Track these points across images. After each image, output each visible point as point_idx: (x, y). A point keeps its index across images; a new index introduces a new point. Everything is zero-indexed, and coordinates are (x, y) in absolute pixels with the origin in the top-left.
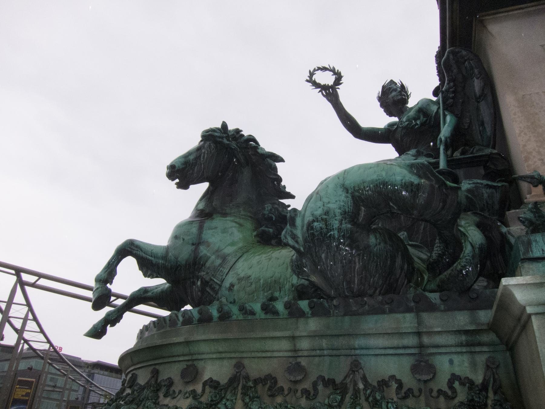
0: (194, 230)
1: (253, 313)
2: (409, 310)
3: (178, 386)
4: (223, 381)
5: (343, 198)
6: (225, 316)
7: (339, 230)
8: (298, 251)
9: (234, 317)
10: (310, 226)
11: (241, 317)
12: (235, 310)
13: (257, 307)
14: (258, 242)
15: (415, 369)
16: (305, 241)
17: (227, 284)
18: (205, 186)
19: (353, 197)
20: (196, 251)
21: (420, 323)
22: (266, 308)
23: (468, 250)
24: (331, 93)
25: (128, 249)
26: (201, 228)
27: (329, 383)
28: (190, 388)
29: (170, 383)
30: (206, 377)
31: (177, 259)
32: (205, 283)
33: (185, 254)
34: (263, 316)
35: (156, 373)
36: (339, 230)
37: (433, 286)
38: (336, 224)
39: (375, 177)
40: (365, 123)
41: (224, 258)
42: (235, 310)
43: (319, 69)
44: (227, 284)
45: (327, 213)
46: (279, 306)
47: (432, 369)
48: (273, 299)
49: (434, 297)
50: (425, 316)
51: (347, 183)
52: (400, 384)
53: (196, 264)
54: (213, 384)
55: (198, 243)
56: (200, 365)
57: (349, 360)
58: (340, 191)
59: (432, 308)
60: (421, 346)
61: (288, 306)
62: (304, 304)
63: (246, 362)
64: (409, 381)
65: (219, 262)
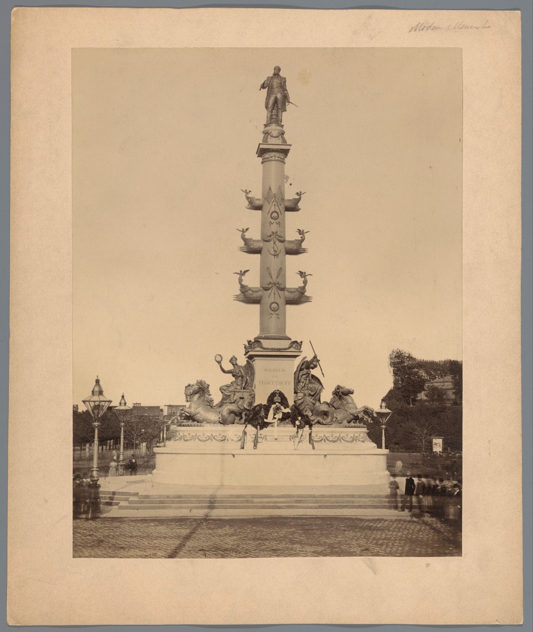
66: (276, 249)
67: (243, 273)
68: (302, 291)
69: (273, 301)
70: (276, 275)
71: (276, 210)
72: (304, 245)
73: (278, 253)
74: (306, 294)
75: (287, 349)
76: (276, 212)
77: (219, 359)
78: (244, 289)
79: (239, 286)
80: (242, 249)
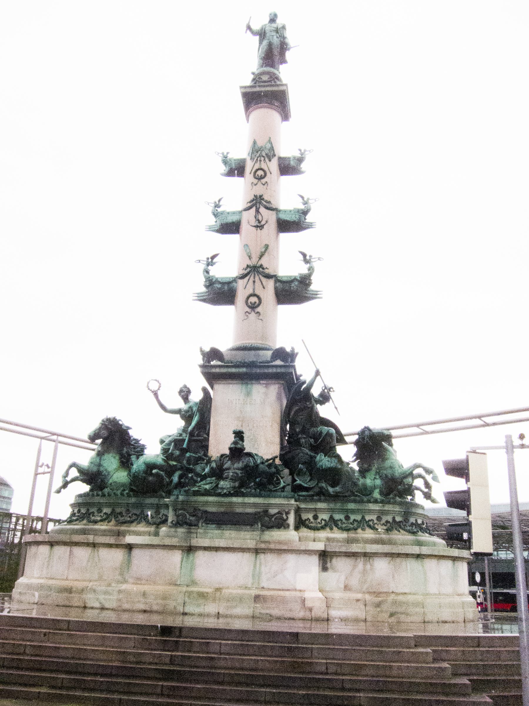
0: (98, 460)
3: (96, 514)
4: (109, 513)
6: (109, 495)
18: (101, 440)
21: (159, 501)
22: (122, 494)
24: (156, 394)
25: (74, 465)
26: (100, 459)
27: (136, 514)
28: (100, 514)
29: (93, 513)
30: (104, 511)
33: (95, 469)
35: (88, 510)
40: (169, 407)
48: (124, 490)
53: (99, 473)
54: (105, 513)
55: (100, 465)
62: (131, 493)
66: (260, 219)
67: (211, 261)
68: (305, 281)
69: (251, 291)
70: (258, 254)
71: (262, 167)
72: (309, 218)
73: (263, 223)
74: (312, 287)
75: (268, 362)
76: (261, 169)
77: (154, 386)
78: (210, 283)
79: (202, 280)
80: (211, 229)
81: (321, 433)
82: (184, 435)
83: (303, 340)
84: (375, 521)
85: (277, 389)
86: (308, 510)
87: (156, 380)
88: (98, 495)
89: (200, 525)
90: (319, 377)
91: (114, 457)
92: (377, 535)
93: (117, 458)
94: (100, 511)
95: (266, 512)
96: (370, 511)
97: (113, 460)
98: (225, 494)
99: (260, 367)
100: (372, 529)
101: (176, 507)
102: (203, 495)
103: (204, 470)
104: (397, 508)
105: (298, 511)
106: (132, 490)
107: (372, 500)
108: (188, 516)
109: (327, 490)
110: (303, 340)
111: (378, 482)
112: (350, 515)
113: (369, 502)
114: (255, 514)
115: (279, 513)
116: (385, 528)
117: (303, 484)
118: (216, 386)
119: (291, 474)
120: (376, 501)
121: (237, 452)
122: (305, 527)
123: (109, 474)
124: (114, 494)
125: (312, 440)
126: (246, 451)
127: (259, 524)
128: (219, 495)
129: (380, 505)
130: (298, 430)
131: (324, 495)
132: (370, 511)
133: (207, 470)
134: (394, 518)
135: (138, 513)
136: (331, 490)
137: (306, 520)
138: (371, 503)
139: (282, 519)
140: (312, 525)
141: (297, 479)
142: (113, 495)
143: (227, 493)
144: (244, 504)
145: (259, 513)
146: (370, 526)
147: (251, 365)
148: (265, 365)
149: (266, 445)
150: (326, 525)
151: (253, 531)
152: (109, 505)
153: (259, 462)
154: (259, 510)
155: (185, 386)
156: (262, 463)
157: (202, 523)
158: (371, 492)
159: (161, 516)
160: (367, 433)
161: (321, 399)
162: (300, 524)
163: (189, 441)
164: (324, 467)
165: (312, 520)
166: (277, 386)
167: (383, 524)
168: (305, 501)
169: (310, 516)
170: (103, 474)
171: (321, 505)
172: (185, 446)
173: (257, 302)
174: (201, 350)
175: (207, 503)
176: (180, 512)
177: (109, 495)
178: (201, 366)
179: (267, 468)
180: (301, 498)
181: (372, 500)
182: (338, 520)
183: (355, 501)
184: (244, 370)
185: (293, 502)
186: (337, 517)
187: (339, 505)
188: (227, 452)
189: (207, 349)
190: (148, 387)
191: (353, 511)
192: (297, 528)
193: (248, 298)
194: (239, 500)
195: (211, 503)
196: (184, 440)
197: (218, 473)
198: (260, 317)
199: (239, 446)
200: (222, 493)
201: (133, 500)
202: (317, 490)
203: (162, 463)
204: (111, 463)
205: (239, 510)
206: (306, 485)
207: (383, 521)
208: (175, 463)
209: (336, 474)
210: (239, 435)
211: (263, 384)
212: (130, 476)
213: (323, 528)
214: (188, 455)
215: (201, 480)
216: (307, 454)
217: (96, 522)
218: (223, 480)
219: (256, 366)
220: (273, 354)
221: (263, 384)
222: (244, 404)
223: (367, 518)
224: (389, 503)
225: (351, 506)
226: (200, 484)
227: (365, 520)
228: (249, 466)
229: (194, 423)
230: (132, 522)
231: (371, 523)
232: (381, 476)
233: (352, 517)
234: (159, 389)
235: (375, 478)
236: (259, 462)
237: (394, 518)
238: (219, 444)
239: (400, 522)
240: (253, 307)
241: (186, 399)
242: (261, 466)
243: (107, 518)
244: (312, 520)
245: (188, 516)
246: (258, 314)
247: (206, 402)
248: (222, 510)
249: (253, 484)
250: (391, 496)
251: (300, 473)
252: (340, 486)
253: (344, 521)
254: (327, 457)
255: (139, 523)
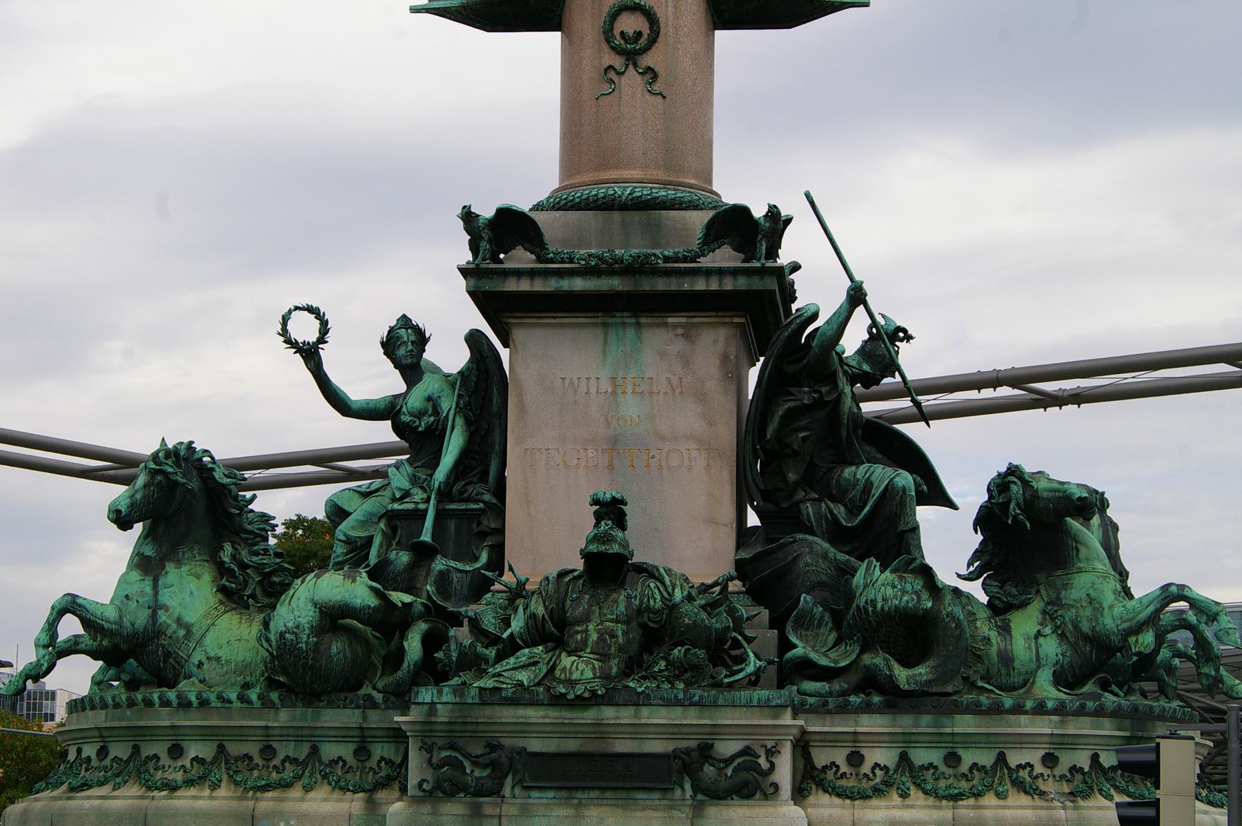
0: (149, 590)
1: (230, 702)
2: (357, 707)
3: (165, 760)
5: (311, 613)
7: (307, 643)
8: (271, 654)
9: (213, 705)
10: (282, 634)
11: (219, 705)
12: (213, 697)
13: (233, 696)
14: (221, 603)
15: (356, 753)
16: (278, 647)
17: (195, 660)
19: (321, 612)
20: (154, 616)
21: (365, 718)
22: (242, 698)
23: (405, 665)
24: (310, 354)
26: (155, 587)
29: (156, 757)
31: (133, 625)
32: (168, 655)
33: (141, 618)
34: (239, 705)
36: (307, 643)
37: (380, 685)
38: (304, 638)
39: (339, 598)
41: (188, 628)
42: (213, 697)
43: (297, 308)
44: (195, 660)
45: (297, 627)
46: (253, 695)
47: (369, 755)
48: (246, 686)
49: (378, 697)
50: (370, 713)
51: (316, 598)
52: (344, 762)
55: (155, 608)
56: (184, 744)
57: (309, 745)
58: (310, 606)
59: (375, 706)
60: (363, 737)
61: (260, 697)
62: (274, 696)
63: (226, 744)
64: (351, 760)
65: (182, 632)
81: (869, 485)
82: (418, 495)
83: (808, 196)
84: (1039, 768)
85: (720, 346)
86: (832, 740)
87: (310, 309)
88: (166, 703)
89: (507, 791)
90: (860, 310)
91: (198, 577)
92: (1043, 813)
93: (207, 577)
94: (176, 751)
95: (706, 751)
96: (1023, 741)
97: (193, 584)
98: (578, 697)
99: (668, 273)
100: (1026, 793)
101: (429, 741)
102: (512, 702)
103: (507, 623)
104: (1107, 728)
105: (803, 745)
106: (272, 683)
107: (1029, 705)
108: (466, 764)
109: (891, 678)
110: (808, 196)
111: (1051, 647)
112: (960, 752)
113: (1018, 709)
114: (675, 754)
115: (747, 751)
116: (1066, 788)
117: (813, 656)
118: (518, 335)
119: (777, 623)
120: (1040, 709)
121: (606, 568)
122: (825, 791)
123: (189, 632)
124: (220, 697)
125: (840, 511)
126: (635, 560)
127: (688, 786)
128: (558, 701)
129: (1055, 718)
130: (792, 477)
131: (881, 692)
132: (1023, 741)
133: (517, 624)
134: (1095, 758)
135: (302, 758)
136: (902, 675)
137: (825, 768)
138: (1026, 713)
139: (756, 767)
140: (843, 782)
141: (794, 639)
142: (215, 703)
143: (587, 695)
144: (637, 731)
145: (687, 752)
146: (1020, 786)
147: (637, 268)
148: (683, 266)
149: (693, 534)
150: (888, 783)
151: (671, 808)
152: (206, 733)
153: (678, 595)
154: (684, 744)
155: (405, 321)
156: (690, 598)
157: (513, 787)
158: (1027, 681)
159: (373, 763)
160: (1016, 489)
161: (866, 367)
162: (809, 780)
163: (440, 516)
164: (879, 606)
165: (844, 768)
166: (722, 333)
167: (1062, 777)
168: (822, 709)
169: (839, 756)
170: (169, 632)
171: (870, 724)
172: (426, 537)
173: (646, 31)
174: (468, 217)
175: (524, 729)
176: (444, 754)
177: (204, 703)
178: (464, 272)
179: (704, 615)
180: (811, 700)
181: (1029, 705)
182: (922, 767)
183: (974, 709)
184: (615, 284)
185: (787, 719)
186: (921, 756)
187: (925, 723)
188: (579, 565)
189: (486, 211)
190: (284, 332)
191: (970, 741)
192: (799, 794)
193: (614, 16)
194: (624, 715)
195: (539, 730)
196: (420, 515)
197: (554, 632)
198: (657, 87)
199: (615, 548)
200: (571, 696)
201: (284, 717)
202: (854, 678)
203: (373, 601)
204: (190, 593)
205: (623, 746)
206: (824, 662)
207: (1063, 768)
208: (408, 598)
209: (921, 629)
210: (611, 511)
211: (676, 326)
212: (268, 640)
213: (878, 792)
214: (439, 564)
215: (500, 658)
216: (825, 556)
217: (173, 788)
218: (570, 654)
219: (656, 272)
220: (710, 226)
221: (676, 326)
222: (614, 393)
223: (1014, 759)
224: (1081, 712)
225: (965, 724)
226: (499, 668)
227: (1009, 768)
228: (648, 609)
229: (448, 458)
230: (287, 785)
231: (1024, 774)
232: (1057, 627)
233: (969, 757)
234: (322, 340)
235: (1039, 634)
236: (678, 595)
237: (1095, 758)
238: (544, 535)
239: (1113, 768)
240: (632, 51)
241: (412, 369)
242: (686, 608)
243: (201, 776)
244: (844, 768)
245: (466, 764)
246: (648, 76)
247: (483, 382)
248: (571, 745)
249: (663, 664)
250: (1089, 688)
251: (805, 623)
252: (930, 663)
253: (943, 768)
254: (887, 573)
255: (308, 789)
